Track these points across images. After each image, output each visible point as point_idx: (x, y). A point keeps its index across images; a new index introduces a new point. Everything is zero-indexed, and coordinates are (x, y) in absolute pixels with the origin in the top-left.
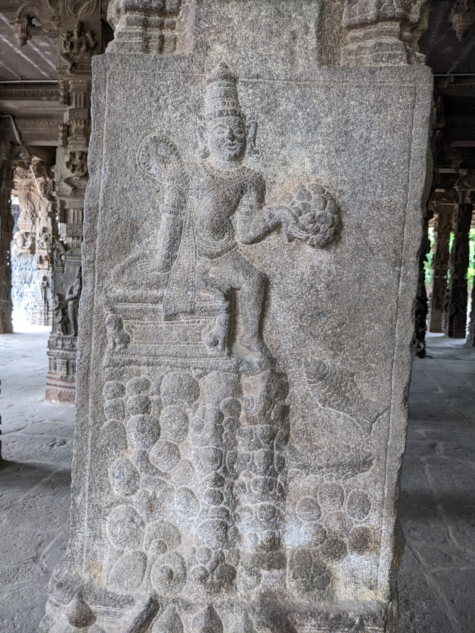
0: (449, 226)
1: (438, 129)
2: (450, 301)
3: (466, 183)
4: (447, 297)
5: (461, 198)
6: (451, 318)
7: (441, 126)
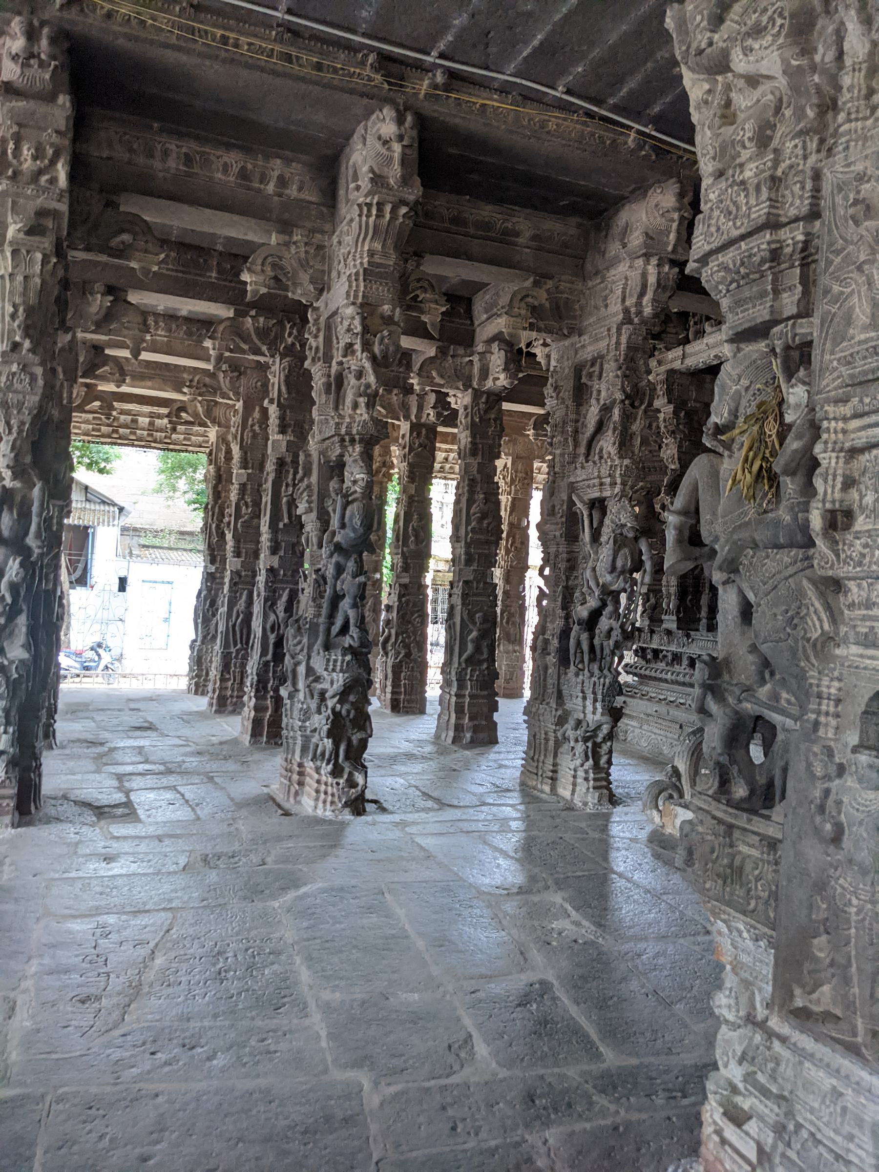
0: (384, 469)
1: (403, 202)
2: (393, 631)
3: (434, 374)
4: (388, 622)
5: (414, 410)
6: (397, 670)
7: (412, 198)
